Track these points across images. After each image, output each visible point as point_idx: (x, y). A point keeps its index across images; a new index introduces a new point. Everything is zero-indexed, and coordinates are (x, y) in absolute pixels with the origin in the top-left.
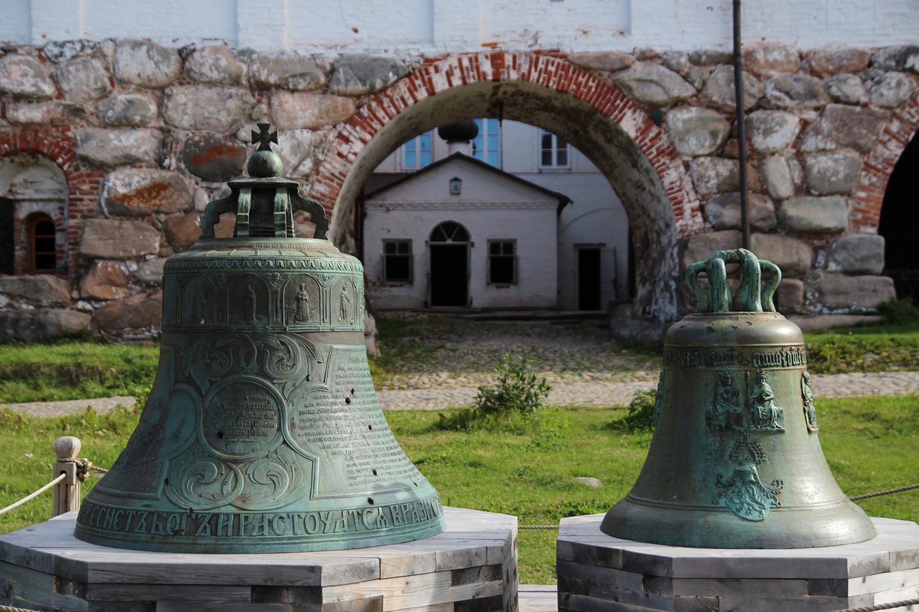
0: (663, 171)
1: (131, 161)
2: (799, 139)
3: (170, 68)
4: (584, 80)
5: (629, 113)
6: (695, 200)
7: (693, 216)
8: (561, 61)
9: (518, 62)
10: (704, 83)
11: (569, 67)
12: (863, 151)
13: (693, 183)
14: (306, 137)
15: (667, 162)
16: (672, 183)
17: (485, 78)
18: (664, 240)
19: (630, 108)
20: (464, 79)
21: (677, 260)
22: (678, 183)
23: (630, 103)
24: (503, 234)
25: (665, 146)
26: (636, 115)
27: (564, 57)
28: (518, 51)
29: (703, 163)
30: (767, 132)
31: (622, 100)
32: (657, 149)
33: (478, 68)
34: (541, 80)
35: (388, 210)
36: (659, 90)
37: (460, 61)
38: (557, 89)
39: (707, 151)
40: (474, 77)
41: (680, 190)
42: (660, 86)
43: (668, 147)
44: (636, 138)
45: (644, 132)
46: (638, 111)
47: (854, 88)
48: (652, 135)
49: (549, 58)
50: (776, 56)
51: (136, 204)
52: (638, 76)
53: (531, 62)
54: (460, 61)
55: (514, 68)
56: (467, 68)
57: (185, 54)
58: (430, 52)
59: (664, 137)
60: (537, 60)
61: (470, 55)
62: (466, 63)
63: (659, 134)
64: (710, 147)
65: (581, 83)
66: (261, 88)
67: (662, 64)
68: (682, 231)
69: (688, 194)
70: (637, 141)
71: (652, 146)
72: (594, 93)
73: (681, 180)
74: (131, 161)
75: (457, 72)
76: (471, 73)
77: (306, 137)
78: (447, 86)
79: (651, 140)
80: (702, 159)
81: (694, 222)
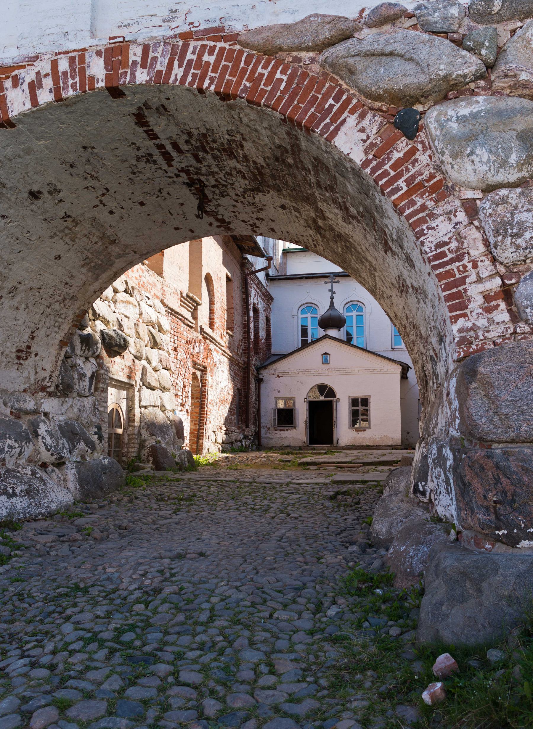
0: (423, 221)
4: (266, 72)
5: (352, 120)
6: (491, 277)
7: (489, 310)
8: (226, 45)
9: (151, 55)
10: (500, 51)
11: (241, 53)
13: (486, 242)
15: (430, 204)
16: (440, 245)
17: (92, 88)
18: (441, 369)
19: (352, 112)
20: (57, 90)
21: (456, 403)
22: (454, 245)
23: (354, 102)
24: (360, 393)
25: (424, 177)
26: (366, 122)
27: (233, 38)
28: (151, 38)
29: (504, 200)
31: (336, 99)
32: (408, 182)
33: (82, 71)
34: (189, 78)
35: (279, 377)
36: (409, 67)
37: (54, 64)
38: (217, 93)
39: (514, 177)
40: (74, 86)
41: (459, 258)
42: (411, 60)
43: (432, 176)
44: (366, 163)
46: (369, 116)
48: (396, 156)
49: (205, 42)
52: (365, 47)
53: (173, 54)
54: (54, 64)
55: (143, 66)
56: (65, 73)
59: (423, 158)
60: (186, 47)
61: (71, 55)
62: (64, 65)
63: (413, 151)
64: (520, 167)
65: (261, 75)
67: (414, 27)
68: (464, 342)
69: (475, 266)
70: (368, 170)
71: (399, 176)
72: (284, 92)
73: (460, 239)
75: (48, 83)
76: (70, 81)
78: (29, 106)
79: (394, 167)
80: (503, 192)
81: (491, 321)
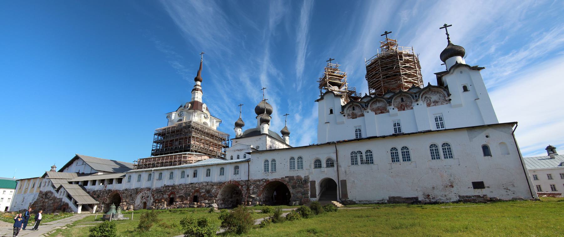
1: (203, 192)
2: (253, 188)
3: (206, 184)
12: (259, 189)
14: (215, 189)
30: (251, 188)
45: (241, 188)
47: (258, 183)
50: (252, 180)
51: (202, 196)
57: (208, 183)
58: (225, 181)
66: (213, 185)
74: (203, 192)
77: (215, 189)
